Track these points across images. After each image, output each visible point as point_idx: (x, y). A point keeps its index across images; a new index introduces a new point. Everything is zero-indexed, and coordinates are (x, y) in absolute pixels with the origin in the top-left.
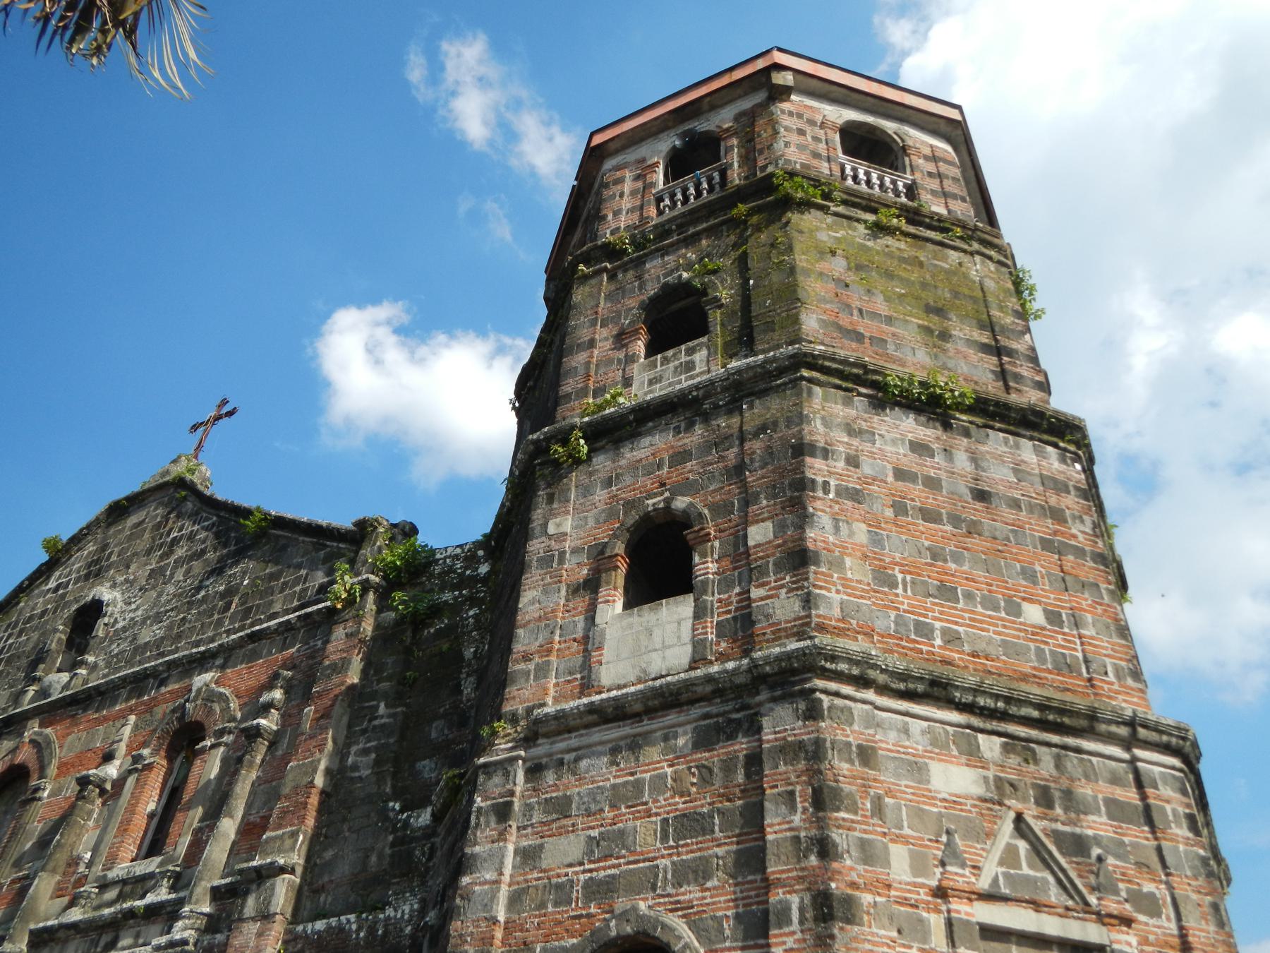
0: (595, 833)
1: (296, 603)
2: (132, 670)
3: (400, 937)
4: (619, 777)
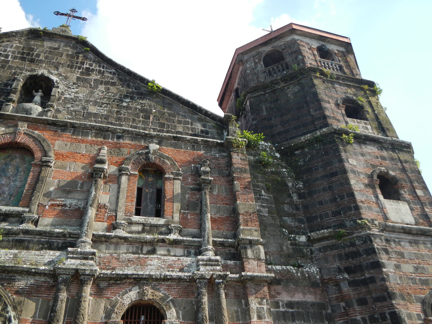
0: (415, 265)
1: (190, 132)
2: (100, 125)
3: (316, 279)
4: (415, 251)
